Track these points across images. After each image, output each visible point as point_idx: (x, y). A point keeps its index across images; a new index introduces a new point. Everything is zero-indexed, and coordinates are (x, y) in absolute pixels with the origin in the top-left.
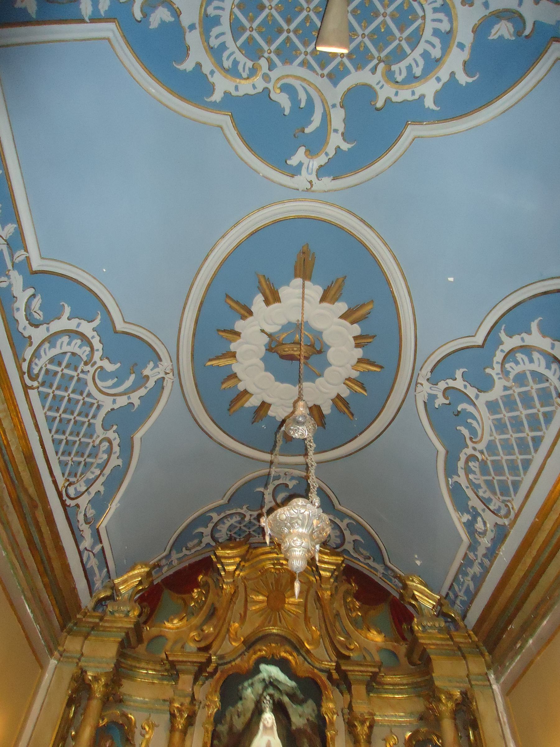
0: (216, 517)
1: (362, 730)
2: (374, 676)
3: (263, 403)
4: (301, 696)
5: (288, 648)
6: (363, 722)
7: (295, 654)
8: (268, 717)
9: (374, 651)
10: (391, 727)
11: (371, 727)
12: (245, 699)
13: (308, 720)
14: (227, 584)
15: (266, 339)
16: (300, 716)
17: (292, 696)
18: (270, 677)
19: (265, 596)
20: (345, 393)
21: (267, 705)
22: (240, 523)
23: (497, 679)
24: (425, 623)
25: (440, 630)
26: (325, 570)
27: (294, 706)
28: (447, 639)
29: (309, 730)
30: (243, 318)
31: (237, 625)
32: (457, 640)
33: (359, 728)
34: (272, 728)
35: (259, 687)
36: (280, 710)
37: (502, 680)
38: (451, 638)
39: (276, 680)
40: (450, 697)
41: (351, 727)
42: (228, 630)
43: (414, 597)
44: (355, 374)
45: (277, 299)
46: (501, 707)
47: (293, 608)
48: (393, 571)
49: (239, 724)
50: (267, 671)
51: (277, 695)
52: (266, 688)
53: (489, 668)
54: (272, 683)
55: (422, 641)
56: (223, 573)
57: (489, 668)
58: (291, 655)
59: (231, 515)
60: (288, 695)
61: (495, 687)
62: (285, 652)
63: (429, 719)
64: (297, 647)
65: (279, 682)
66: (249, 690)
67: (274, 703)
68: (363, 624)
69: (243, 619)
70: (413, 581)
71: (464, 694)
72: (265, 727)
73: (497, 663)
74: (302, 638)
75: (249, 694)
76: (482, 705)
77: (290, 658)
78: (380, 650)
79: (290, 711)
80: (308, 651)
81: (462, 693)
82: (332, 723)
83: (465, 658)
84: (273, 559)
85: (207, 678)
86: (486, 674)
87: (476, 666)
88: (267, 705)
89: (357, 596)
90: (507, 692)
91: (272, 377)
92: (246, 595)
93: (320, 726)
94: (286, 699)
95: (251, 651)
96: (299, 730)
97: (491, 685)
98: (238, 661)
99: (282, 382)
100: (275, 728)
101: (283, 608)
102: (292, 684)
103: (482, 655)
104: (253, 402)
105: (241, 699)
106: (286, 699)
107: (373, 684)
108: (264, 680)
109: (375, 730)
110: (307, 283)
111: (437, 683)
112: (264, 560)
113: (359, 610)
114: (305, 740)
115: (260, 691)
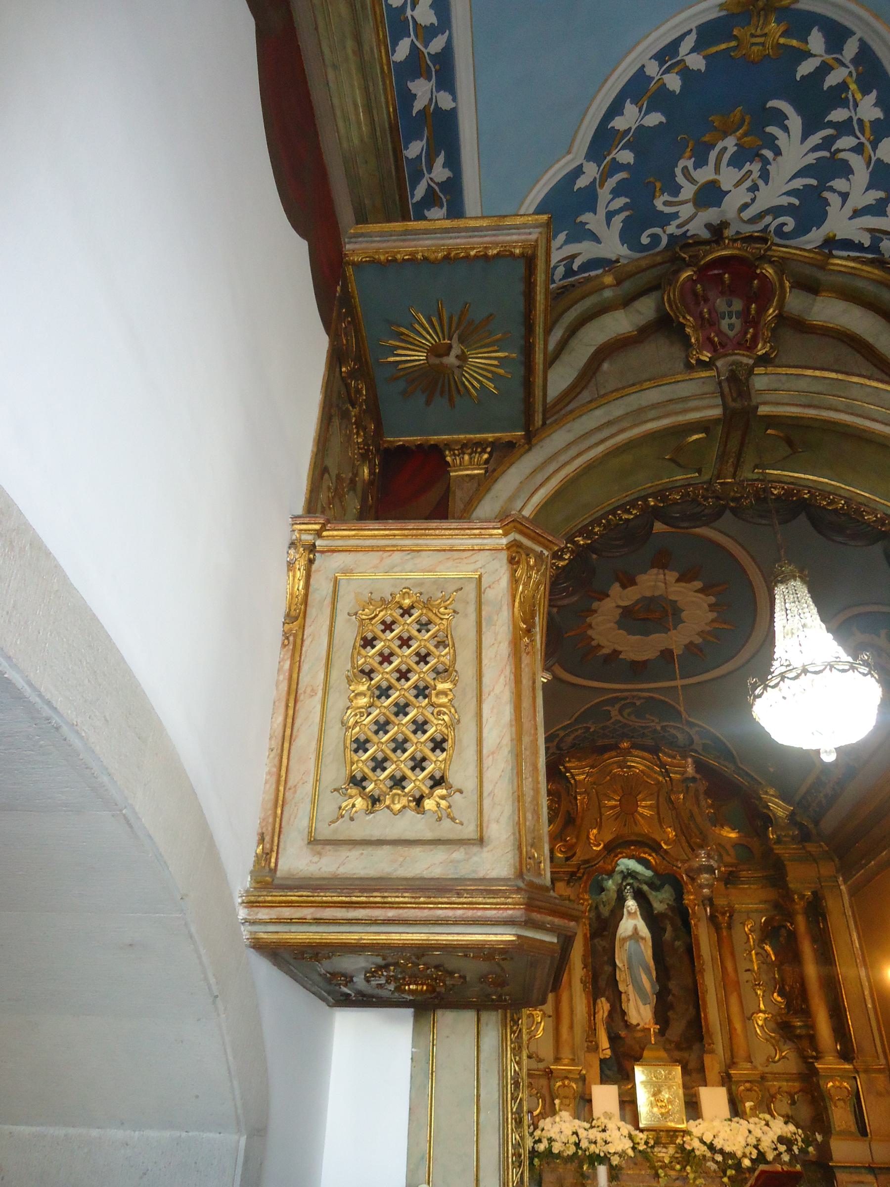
0: (562, 734)
1: (723, 920)
2: (731, 873)
3: (615, 651)
4: (658, 883)
5: (646, 849)
6: (723, 914)
7: (654, 854)
8: (631, 904)
9: (728, 847)
10: (748, 912)
11: (731, 917)
12: (608, 890)
13: (668, 904)
14: (580, 794)
15: (620, 610)
16: (661, 901)
17: (651, 885)
18: (628, 869)
19: (616, 800)
20: (698, 640)
21: (628, 892)
22: (584, 733)
23: (845, 881)
24: (779, 833)
25: (793, 838)
26: (675, 773)
27: (654, 893)
28: (801, 849)
29: (670, 913)
30: (600, 600)
31: (595, 831)
32: (809, 849)
33: (720, 918)
34: (635, 913)
35: (618, 878)
36: (640, 896)
37: (849, 883)
38: (804, 848)
39: (634, 871)
40: (802, 897)
41: (712, 919)
42: (588, 838)
43: (768, 807)
44: (708, 628)
45: (633, 583)
46: (847, 904)
47: (647, 812)
48: (743, 770)
49: (605, 911)
50: (624, 864)
51: (636, 884)
52: (624, 878)
53: (837, 872)
54: (631, 874)
55: (777, 852)
56: (572, 781)
57: (837, 872)
58: (650, 855)
59: (577, 730)
60: (646, 883)
61: (843, 887)
62: (645, 853)
63: (782, 907)
64: (655, 847)
65: (638, 873)
66: (610, 882)
67: (634, 892)
68: (718, 821)
69: (600, 827)
70: (766, 793)
71: (815, 893)
72: (629, 913)
73: (846, 869)
74: (658, 839)
75: (610, 884)
76: (831, 903)
77: (650, 858)
78: (736, 845)
79: (651, 898)
80: (665, 851)
81: (813, 893)
82: (694, 912)
83: (817, 863)
84: (619, 761)
85: (576, 880)
86: (836, 877)
87: (827, 869)
88: (628, 892)
89: (708, 794)
90: (853, 893)
91: (625, 633)
92: (599, 801)
93: (681, 914)
94: (645, 888)
95: (613, 855)
96: (662, 915)
97: (839, 886)
98: (600, 864)
99: (634, 635)
100: (638, 913)
101: (636, 811)
102: (649, 873)
103: (833, 861)
104: (606, 651)
105: (603, 890)
106: (645, 888)
107: (730, 879)
108: (622, 872)
109: (735, 916)
110: (666, 571)
111: (791, 886)
112: (610, 764)
113: (711, 806)
114: (668, 922)
115: (620, 881)
